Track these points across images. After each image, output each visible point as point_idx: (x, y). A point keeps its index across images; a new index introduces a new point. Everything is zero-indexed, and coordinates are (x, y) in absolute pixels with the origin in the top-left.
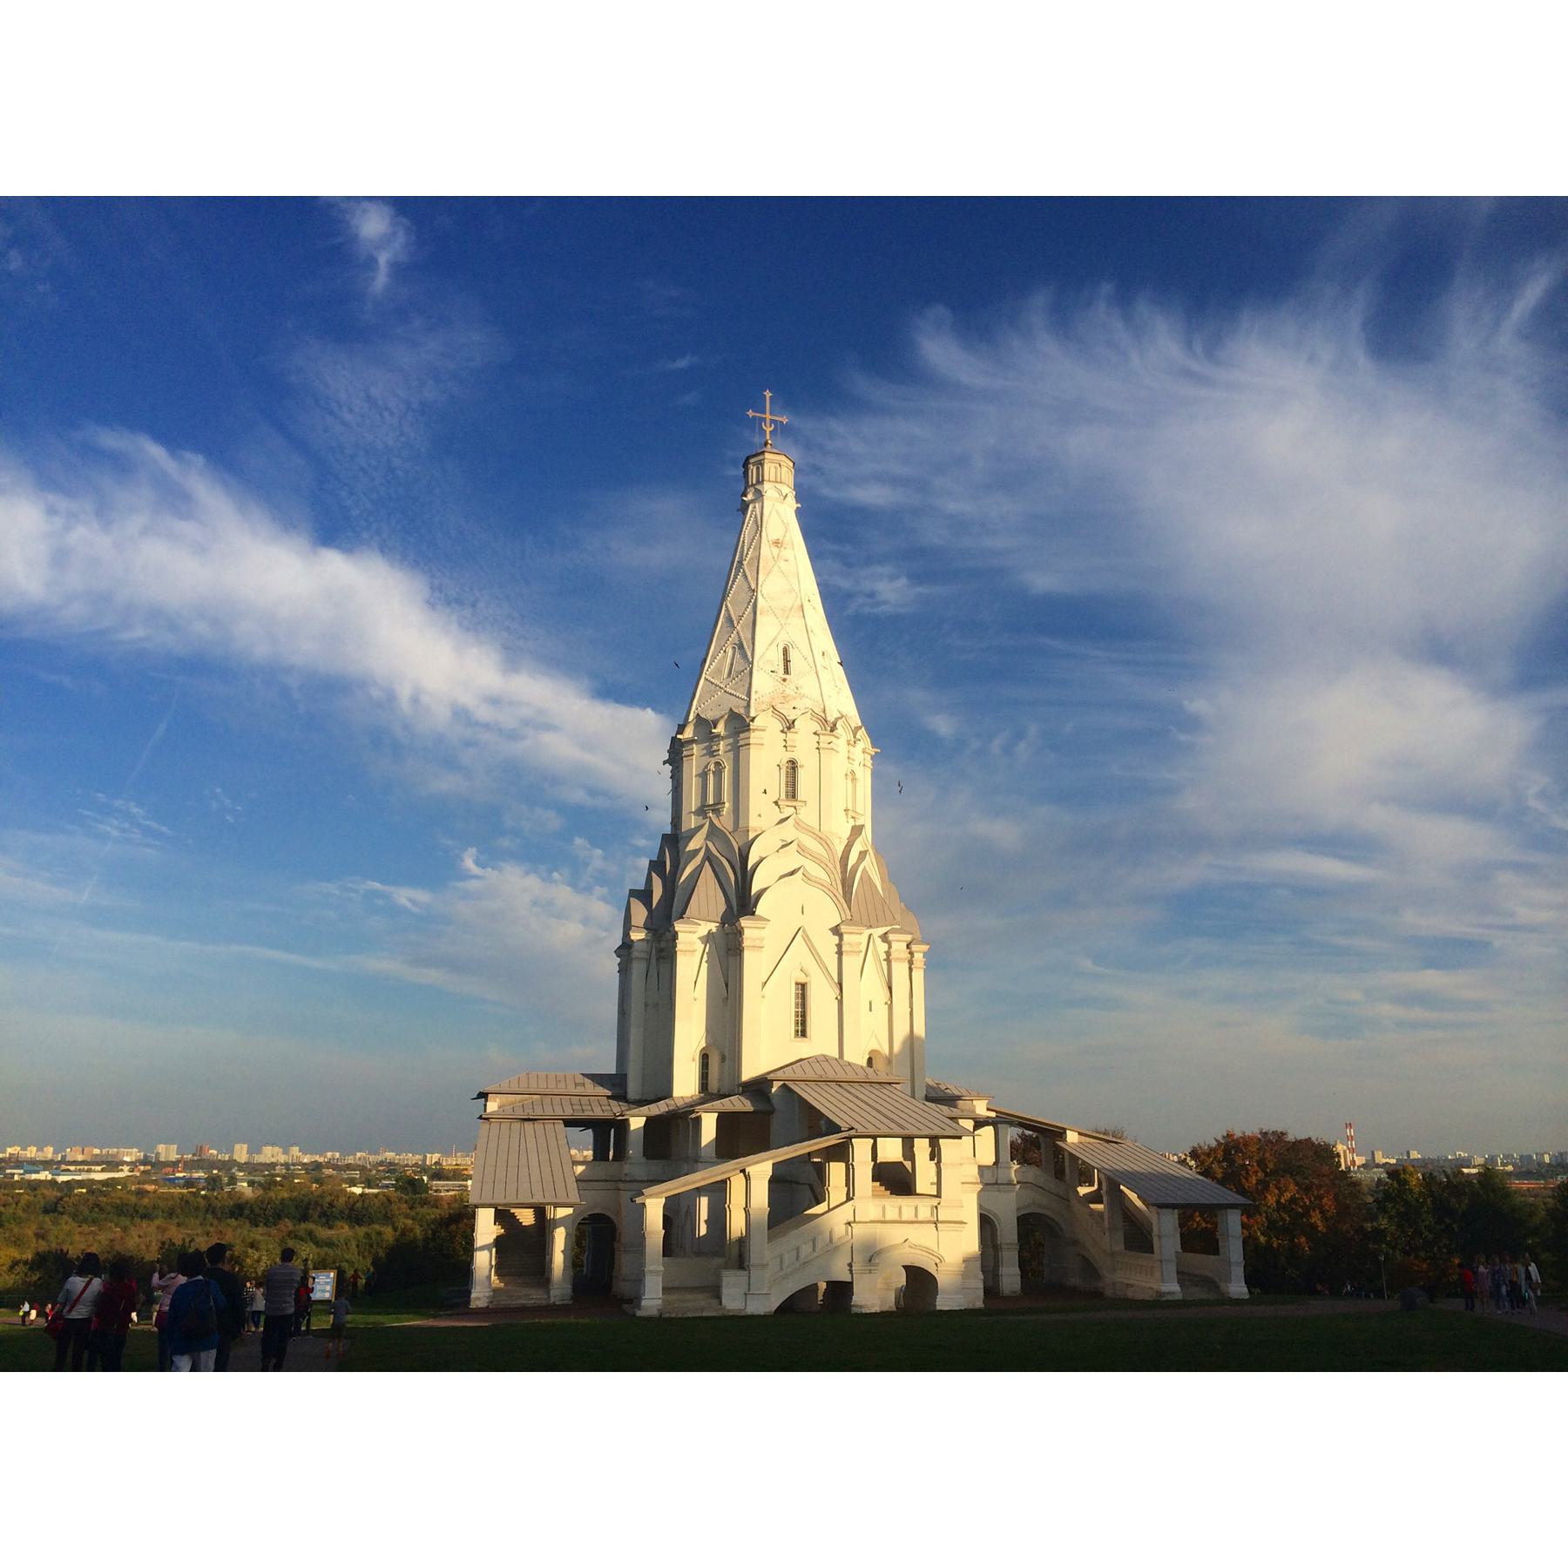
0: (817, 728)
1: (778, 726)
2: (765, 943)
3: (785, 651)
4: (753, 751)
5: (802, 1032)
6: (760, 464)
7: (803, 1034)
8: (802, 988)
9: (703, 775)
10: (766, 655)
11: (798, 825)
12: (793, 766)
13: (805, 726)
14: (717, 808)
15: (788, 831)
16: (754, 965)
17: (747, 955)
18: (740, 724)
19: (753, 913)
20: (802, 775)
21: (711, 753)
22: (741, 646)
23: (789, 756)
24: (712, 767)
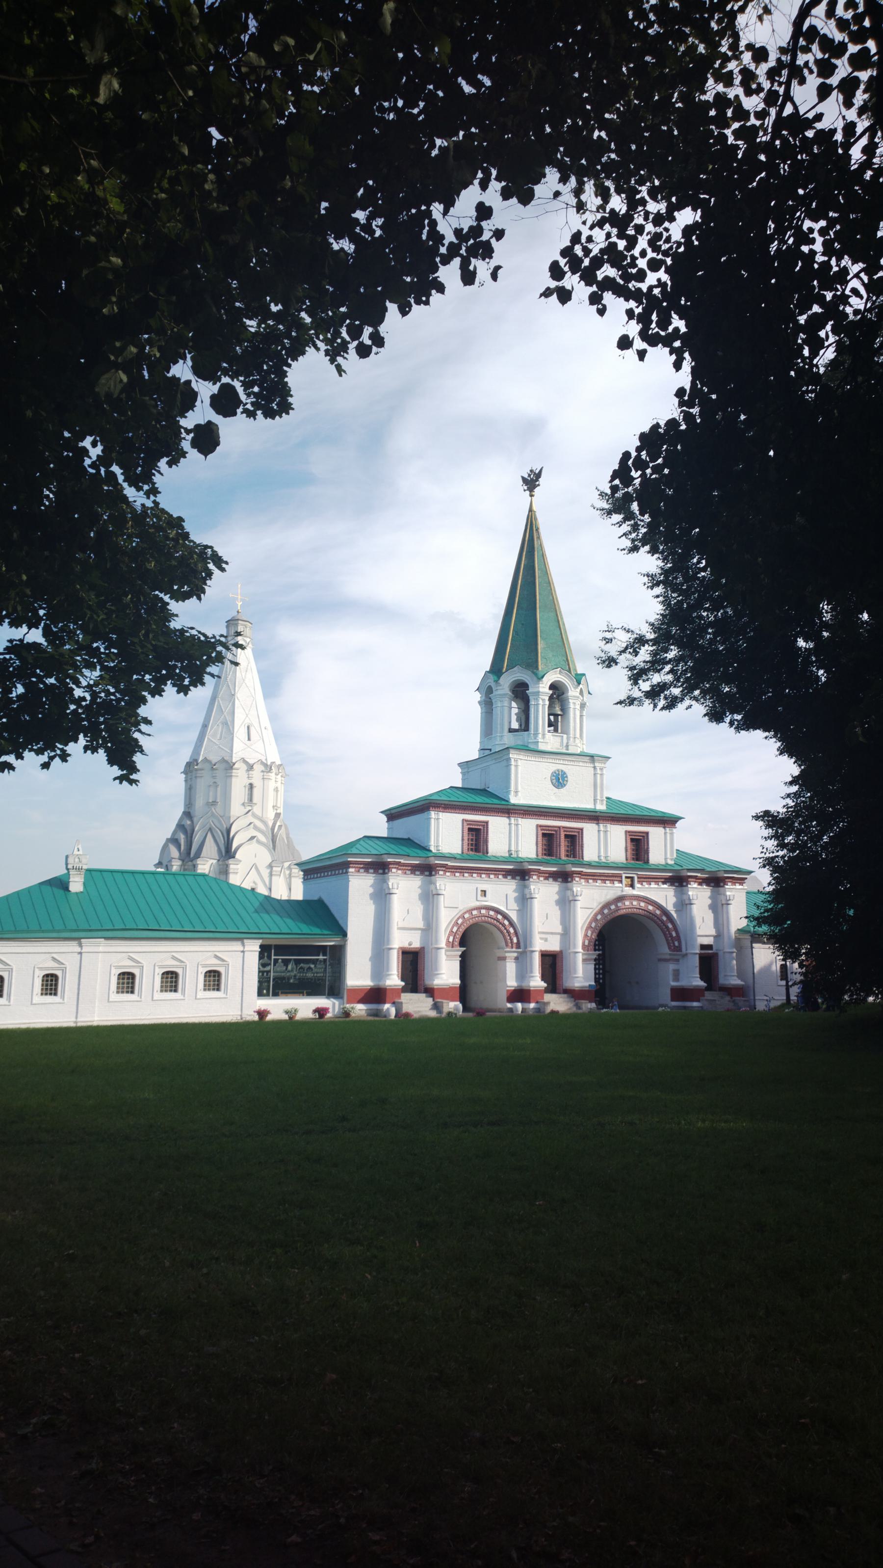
1: (245, 767)
3: (248, 728)
4: (234, 780)
10: (240, 733)
11: (254, 816)
12: (251, 786)
13: (258, 768)
14: (214, 803)
15: (250, 818)
18: (229, 766)
19: (234, 857)
20: (255, 791)
22: (227, 724)
23: (250, 781)
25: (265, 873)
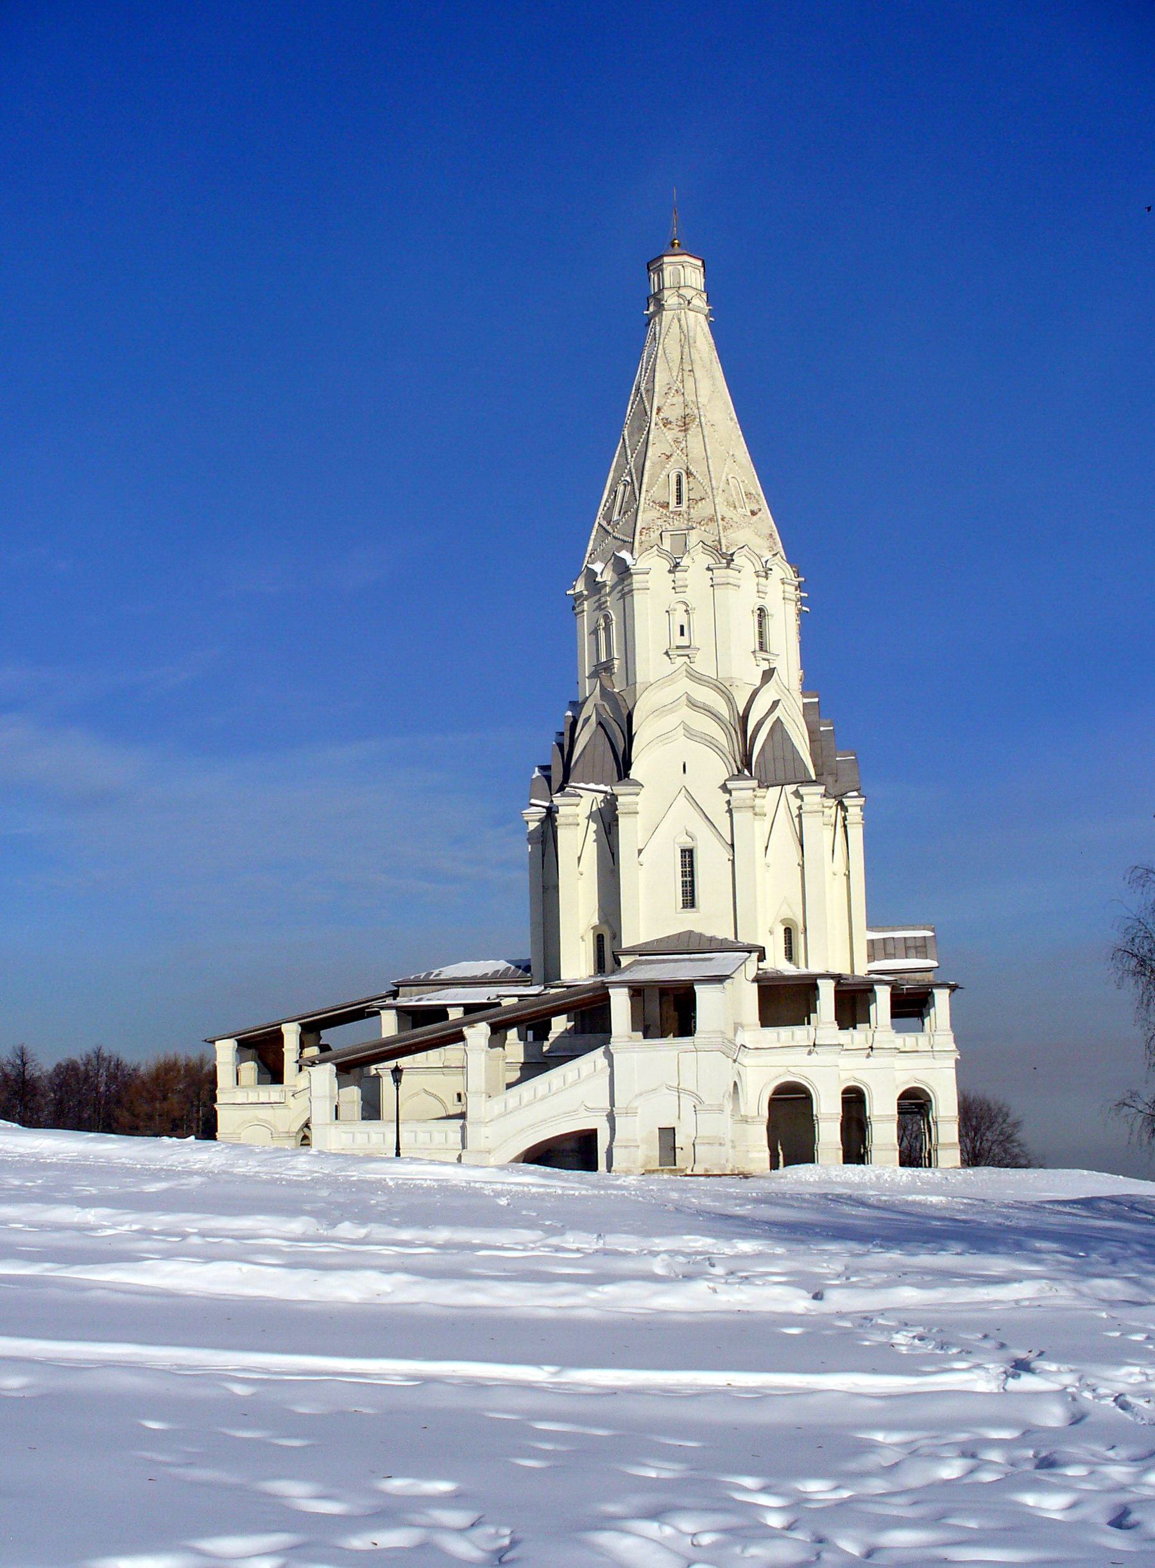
0: (710, 561)
2: (639, 809)
4: (637, 596)
5: (690, 901)
6: (660, 270)
7: (693, 905)
8: (688, 855)
9: (595, 632)
16: (629, 832)
17: (622, 821)
21: (601, 607)
24: (602, 621)
25: (716, 804)
